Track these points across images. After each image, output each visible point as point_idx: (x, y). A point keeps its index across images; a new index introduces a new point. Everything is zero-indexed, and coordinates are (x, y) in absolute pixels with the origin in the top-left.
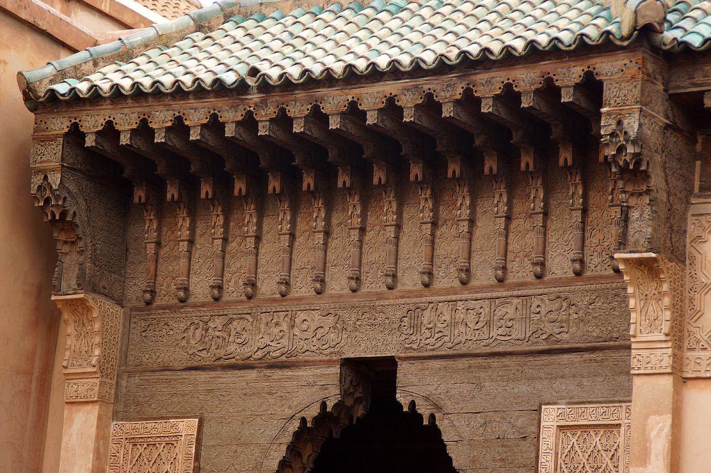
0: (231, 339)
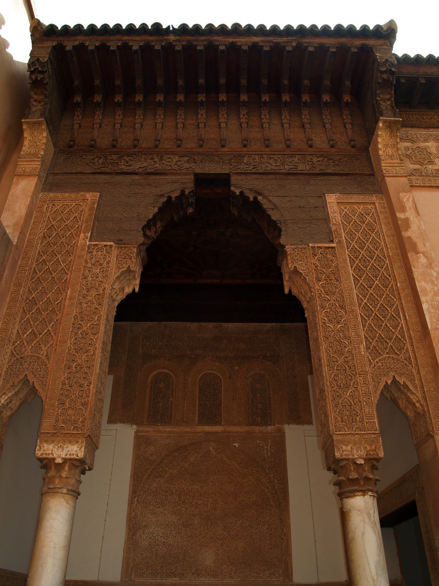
0: (122, 163)
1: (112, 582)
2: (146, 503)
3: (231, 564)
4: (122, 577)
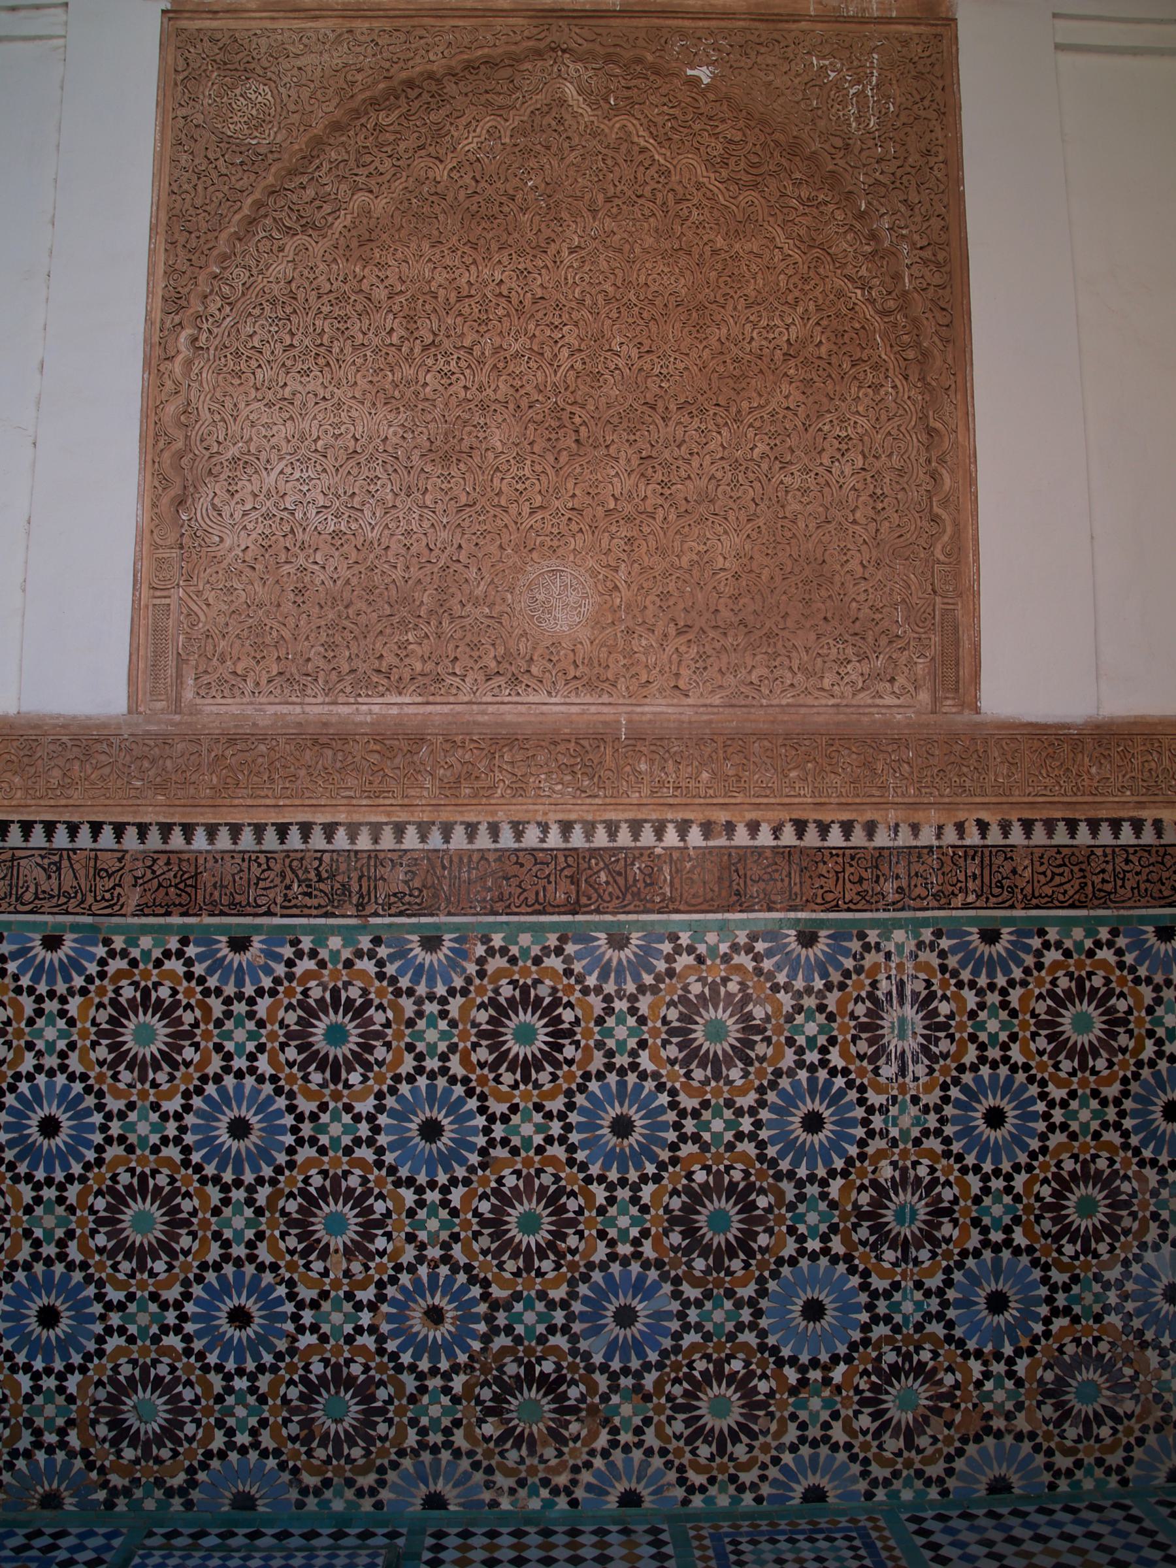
1: (89, 718)
2: (237, 354)
3: (680, 633)
4: (133, 696)
